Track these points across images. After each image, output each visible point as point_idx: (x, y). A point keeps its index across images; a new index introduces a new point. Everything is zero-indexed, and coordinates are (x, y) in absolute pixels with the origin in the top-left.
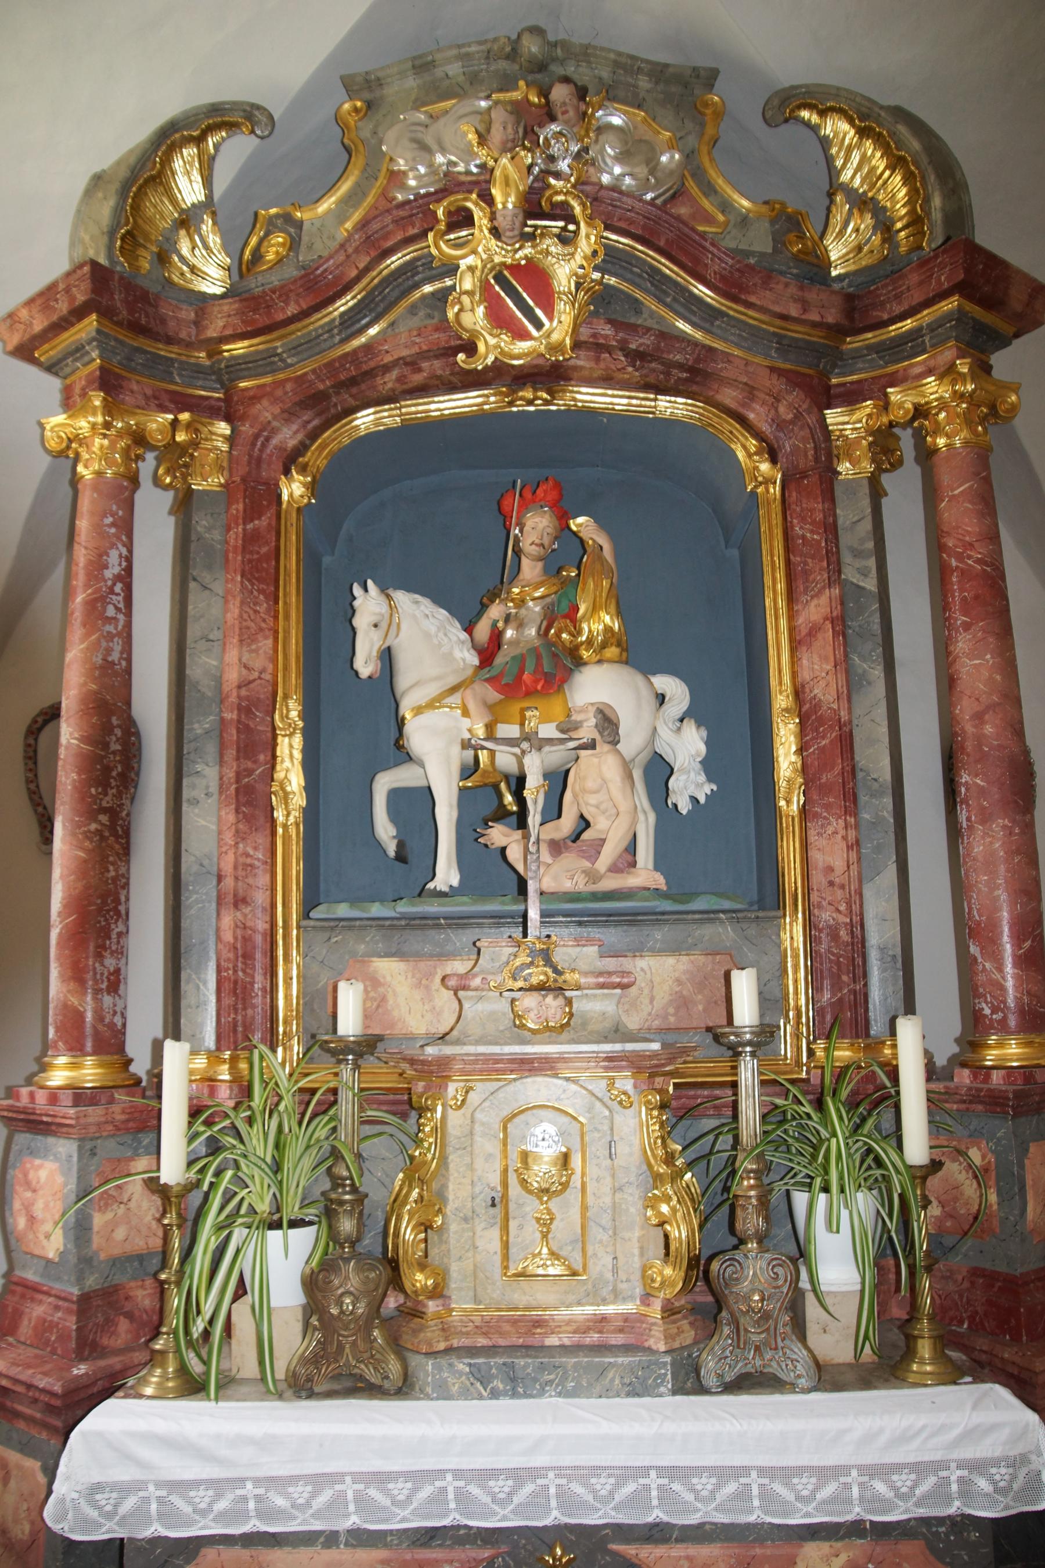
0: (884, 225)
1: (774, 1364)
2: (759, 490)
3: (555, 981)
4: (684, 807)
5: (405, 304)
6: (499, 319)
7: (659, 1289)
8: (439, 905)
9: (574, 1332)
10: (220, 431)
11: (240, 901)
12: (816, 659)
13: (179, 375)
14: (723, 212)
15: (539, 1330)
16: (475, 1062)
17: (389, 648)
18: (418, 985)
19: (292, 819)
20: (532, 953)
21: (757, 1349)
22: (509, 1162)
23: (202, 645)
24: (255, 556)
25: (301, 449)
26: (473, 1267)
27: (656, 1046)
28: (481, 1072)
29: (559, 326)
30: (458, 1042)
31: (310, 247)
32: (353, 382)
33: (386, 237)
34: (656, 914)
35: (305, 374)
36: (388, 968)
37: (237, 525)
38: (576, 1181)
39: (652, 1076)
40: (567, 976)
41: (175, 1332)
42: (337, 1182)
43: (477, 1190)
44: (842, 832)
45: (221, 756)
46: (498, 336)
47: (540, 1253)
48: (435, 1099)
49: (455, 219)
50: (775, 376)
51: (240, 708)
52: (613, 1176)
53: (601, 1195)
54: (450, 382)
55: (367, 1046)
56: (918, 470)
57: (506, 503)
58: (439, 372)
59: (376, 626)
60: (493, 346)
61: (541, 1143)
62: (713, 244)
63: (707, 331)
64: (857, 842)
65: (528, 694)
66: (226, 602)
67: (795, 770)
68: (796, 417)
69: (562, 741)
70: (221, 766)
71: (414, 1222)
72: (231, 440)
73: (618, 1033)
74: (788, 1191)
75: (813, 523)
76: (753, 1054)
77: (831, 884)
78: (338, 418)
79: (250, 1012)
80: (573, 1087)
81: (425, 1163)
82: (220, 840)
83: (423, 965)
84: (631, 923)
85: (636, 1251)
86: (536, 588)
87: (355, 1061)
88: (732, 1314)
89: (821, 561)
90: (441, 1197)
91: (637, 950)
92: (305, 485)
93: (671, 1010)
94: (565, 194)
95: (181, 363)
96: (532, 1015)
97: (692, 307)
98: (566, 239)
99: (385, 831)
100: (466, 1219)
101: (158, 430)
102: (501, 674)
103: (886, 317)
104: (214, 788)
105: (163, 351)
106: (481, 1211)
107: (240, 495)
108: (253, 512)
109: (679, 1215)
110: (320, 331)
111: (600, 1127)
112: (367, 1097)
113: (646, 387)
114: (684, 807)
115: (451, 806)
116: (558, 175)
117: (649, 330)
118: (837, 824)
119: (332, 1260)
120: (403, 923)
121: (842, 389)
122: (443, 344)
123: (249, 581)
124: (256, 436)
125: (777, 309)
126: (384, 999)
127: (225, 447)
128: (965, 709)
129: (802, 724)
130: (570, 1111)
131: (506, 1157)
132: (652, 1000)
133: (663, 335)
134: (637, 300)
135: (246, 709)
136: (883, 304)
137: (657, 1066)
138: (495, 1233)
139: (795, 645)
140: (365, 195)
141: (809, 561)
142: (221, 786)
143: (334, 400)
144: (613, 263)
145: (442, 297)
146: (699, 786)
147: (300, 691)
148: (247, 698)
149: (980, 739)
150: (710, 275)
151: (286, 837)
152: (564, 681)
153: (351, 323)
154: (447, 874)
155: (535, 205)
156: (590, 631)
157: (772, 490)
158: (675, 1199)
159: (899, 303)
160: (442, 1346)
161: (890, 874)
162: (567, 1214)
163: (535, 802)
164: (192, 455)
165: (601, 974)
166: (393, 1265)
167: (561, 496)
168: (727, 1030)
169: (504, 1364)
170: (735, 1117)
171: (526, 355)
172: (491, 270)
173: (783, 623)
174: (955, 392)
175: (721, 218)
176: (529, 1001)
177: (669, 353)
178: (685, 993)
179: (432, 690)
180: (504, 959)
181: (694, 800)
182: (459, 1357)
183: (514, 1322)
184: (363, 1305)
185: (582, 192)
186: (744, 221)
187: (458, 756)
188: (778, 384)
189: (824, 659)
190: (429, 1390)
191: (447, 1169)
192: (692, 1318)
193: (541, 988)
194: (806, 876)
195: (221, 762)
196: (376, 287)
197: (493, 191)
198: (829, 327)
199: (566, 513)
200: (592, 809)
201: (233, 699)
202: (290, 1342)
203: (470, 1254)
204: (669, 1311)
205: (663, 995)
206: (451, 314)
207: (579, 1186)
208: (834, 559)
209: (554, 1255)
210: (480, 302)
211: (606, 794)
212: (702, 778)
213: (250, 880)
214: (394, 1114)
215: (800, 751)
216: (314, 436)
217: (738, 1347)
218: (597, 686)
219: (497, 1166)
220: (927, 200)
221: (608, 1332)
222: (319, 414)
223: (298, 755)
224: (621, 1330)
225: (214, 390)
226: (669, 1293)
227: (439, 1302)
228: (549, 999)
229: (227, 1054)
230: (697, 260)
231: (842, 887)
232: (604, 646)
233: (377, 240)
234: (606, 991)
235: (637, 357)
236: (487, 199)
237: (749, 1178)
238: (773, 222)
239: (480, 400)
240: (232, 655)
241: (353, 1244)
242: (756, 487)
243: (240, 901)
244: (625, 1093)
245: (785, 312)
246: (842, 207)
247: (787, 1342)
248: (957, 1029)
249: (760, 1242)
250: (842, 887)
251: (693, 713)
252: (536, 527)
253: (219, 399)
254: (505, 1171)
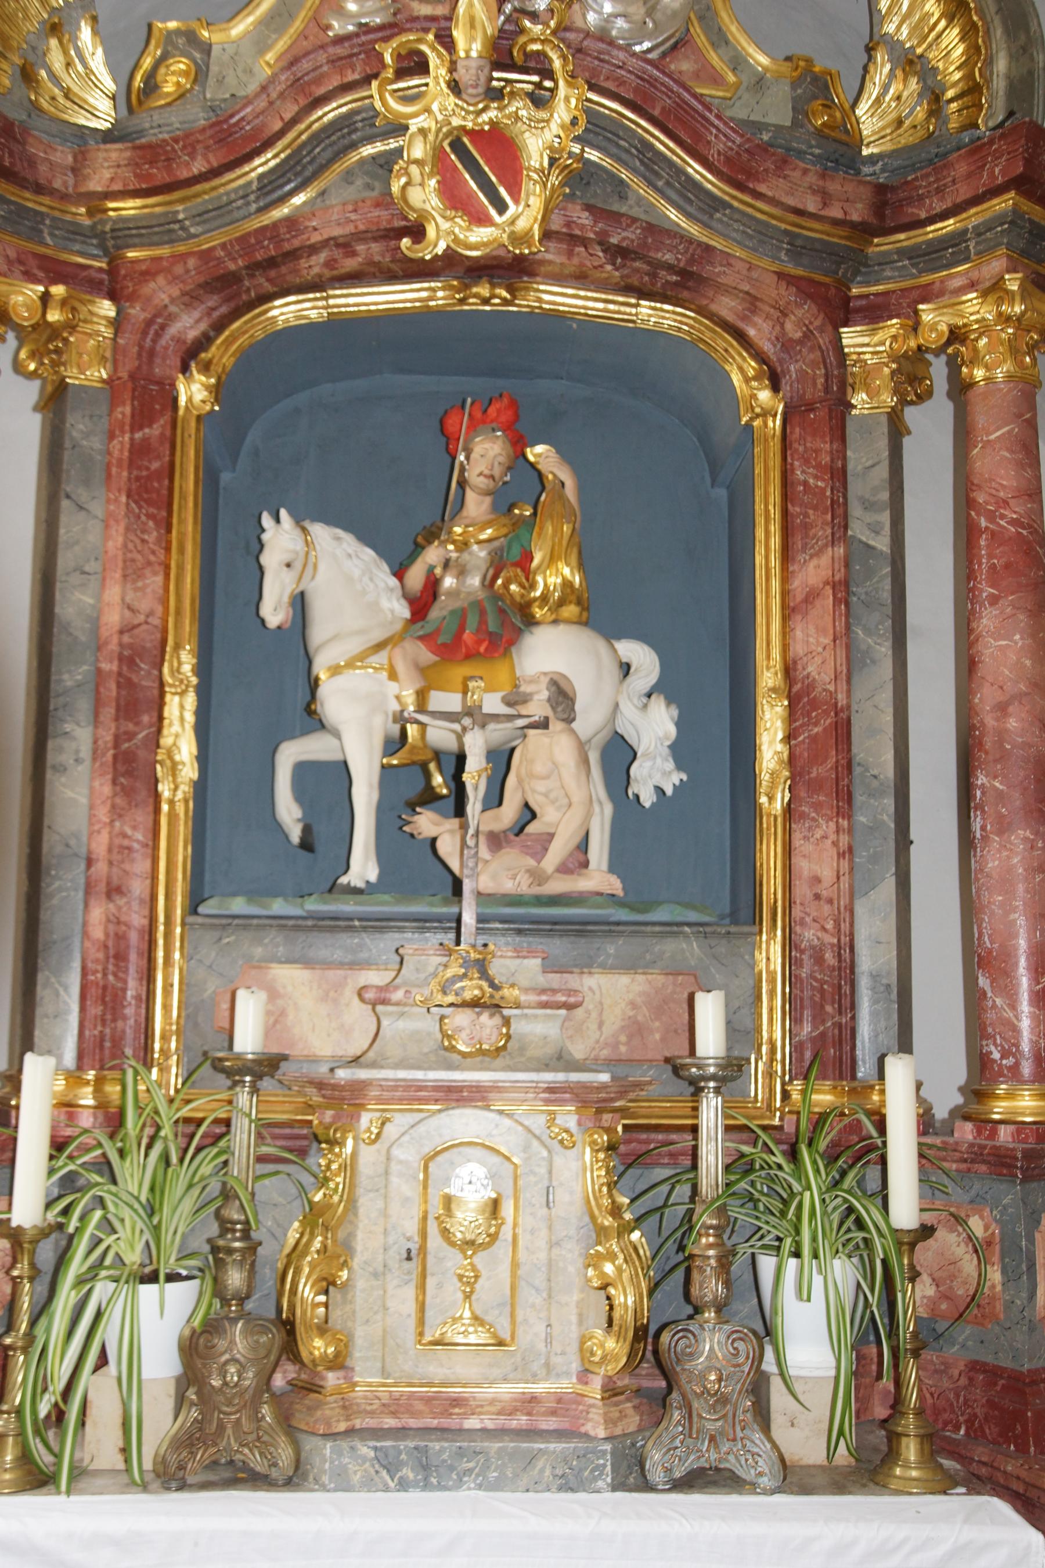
0: (934, 96)
1: (731, 1457)
2: (755, 424)
3: (492, 996)
4: (648, 799)
5: (339, 168)
6: (454, 199)
7: (600, 1364)
8: (356, 904)
9: (499, 1414)
10: (103, 312)
11: (114, 891)
12: (812, 630)
13: (51, 235)
14: (734, 70)
15: (457, 1410)
16: (395, 1088)
17: (302, 594)
18: (324, 998)
19: (180, 795)
20: (466, 963)
21: (712, 1439)
22: (430, 1209)
23: (76, 579)
24: (144, 473)
25: (204, 342)
26: (383, 1333)
27: (605, 1077)
28: (400, 1101)
29: (524, 214)
30: (373, 1065)
31: (220, 81)
32: (271, 263)
33: (318, 81)
34: (609, 923)
35: (212, 249)
36: (290, 977)
37: (123, 432)
38: (506, 1232)
39: (599, 1111)
40: (506, 992)
41: (19, 1411)
42: (226, 1226)
43: (391, 1240)
44: (833, 837)
45: (96, 714)
46: (452, 219)
47: (461, 1317)
48: (345, 1132)
49: (405, 64)
50: (784, 284)
51: (121, 658)
52: (550, 1228)
53: (534, 1250)
54: (389, 270)
55: (268, 1065)
56: (949, 407)
57: (451, 422)
58: (377, 258)
59: (288, 565)
60: (445, 232)
61: (467, 1187)
62: (719, 117)
63: (706, 225)
64: (850, 849)
65: (469, 656)
66: (107, 527)
67: (781, 762)
68: (805, 336)
69: (510, 718)
70: (96, 727)
71: (314, 1277)
72: (117, 324)
73: (561, 1061)
74: (753, 1255)
75: (818, 466)
76: (717, 1091)
77: (817, 897)
78: (251, 306)
79: (120, 1024)
80: (507, 1122)
81: (330, 1206)
82: (91, 817)
83: (333, 975)
84: (580, 933)
85: (574, 1319)
86: (483, 529)
87: (253, 1083)
88: (684, 1396)
89: (825, 513)
90: (348, 1248)
91: (586, 965)
92: (207, 387)
93: (623, 1038)
94: (543, 42)
95: (54, 219)
96: (464, 1035)
97: (688, 194)
98: (540, 100)
99: (289, 812)
100: (375, 1275)
101: (25, 305)
102: (437, 632)
103: (923, 215)
104: (86, 752)
105: (30, 201)
106: (394, 1264)
107: (127, 395)
108: (142, 418)
109: (625, 1276)
110: (233, 196)
111: (537, 1170)
112: (265, 1129)
113: (627, 289)
114: (648, 799)
115: (371, 786)
116: (534, 16)
117: (634, 220)
118: (826, 827)
119: (216, 1320)
120: (310, 923)
121: (864, 302)
122: (384, 225)
123: (136, 502)
124: (149, 323)
125: (791, 201)
126: (283, 1013)
127: (108, 332)
128: (986, 698)
129: (791, 708)
130: (503, 1150)
131: (426, 1202)
132: (601, 1025)
133: (651, 229)
134: (622, 182)
135: (128, 659)
136: (921, 198)
137: (605, 1100)
138: (410, 1293)
139: (788, 612)
140: (292, 17)
141: (811, 512)
142: (95, 751)
143: (247, 283)
144: (597, 134)
145: (386, 163)
146: (666, 774)
147: (195, 640)
148: (131, 646)
149: (1001, 735)
150: (712, 155)
151: (172, 815)
152: (512, 643)
153: (272, 189)
154: (363, 867)
155: (503, 54)
156: (546, 585)
157: (771, 424)
158: (621, 1257)
159: (942, 199)
160: (342, 1427)
161: (888, 887)
162: (494, 1269)
163: (476, 788)
164: (66, 341)
165: (543, 991)
166: (288, 1327)
167: (517, 417)
168: (688, 1061)
169: (416, 1448)
170: (695, 1167)
171: (485, 245)
172: (446, 136)
173: (775, 585)
174: (1000, 314)
175: (731, 78)
176: (462, 1019)
177: (658, 250)
178: (640, 1018)
179: (354, 646)
180: (431, 969)
181: (660, 791)
182: (363, 1439)
183: (428, 1400)
184: (251, 1375)
185: (563, 40)
186: (759, 83)
187: (382, 726)
188: (787, 295)
189: (821, 631)
190: (325, 1479)
191: (356, 1215)
192: (637, 1401)
193: (474, 1004)
194: (788, 886)
195: (96, 722)
196: (304, 145)
197: (455, 33)
198: (853, 226)
199: (522, 437)
200: (540, 799)
201: (113, 646)
202: (160, 1422)
203: (379, 1317)
204: (611, 1391)
205: (614, 1020)
206: (395, 188)
207: (510, 1239)
208: (840, 511)
209: (477, 1319)
210: (431, 175)
211: (557, 780)
212: (670, 765)
213: (127, 866)
214: (291, 1150)
215: (788, 738)
216: (219, 327)
217: (690, 1436)
218: (551, 651)
219: (416, 1213)
220: (989, 62)
221: (538, 1414)
222: (227, 300)
223: (190, 718)
224: (554, 1413)
225: (94, 257)
226: (612, 1368)
227: (340, 1374)
228: (485, 1017)
229: (91, 1075)
230: (698, 137)
231: (830, 901)
232: (561, 603)
233: (309, 84)
234: (549, 1011)
235: (619, 253)
236: (446, 41)
237: (709, 1235)
238: (795, 84)
239: (424, 294)
240: (113, 593)
241: (242, 1300)
242: (752, 419)
243: (114, 891)
244: (567, 1131)
245: (800, 206)
246: (882, 68)
247: (747, 1432)
248: (961, 1077)
249: (718, 1311)
250: (830, 901)
251: (664, 688)
252: (485, 455)
253: (100, 270)
254: (425, 1218)
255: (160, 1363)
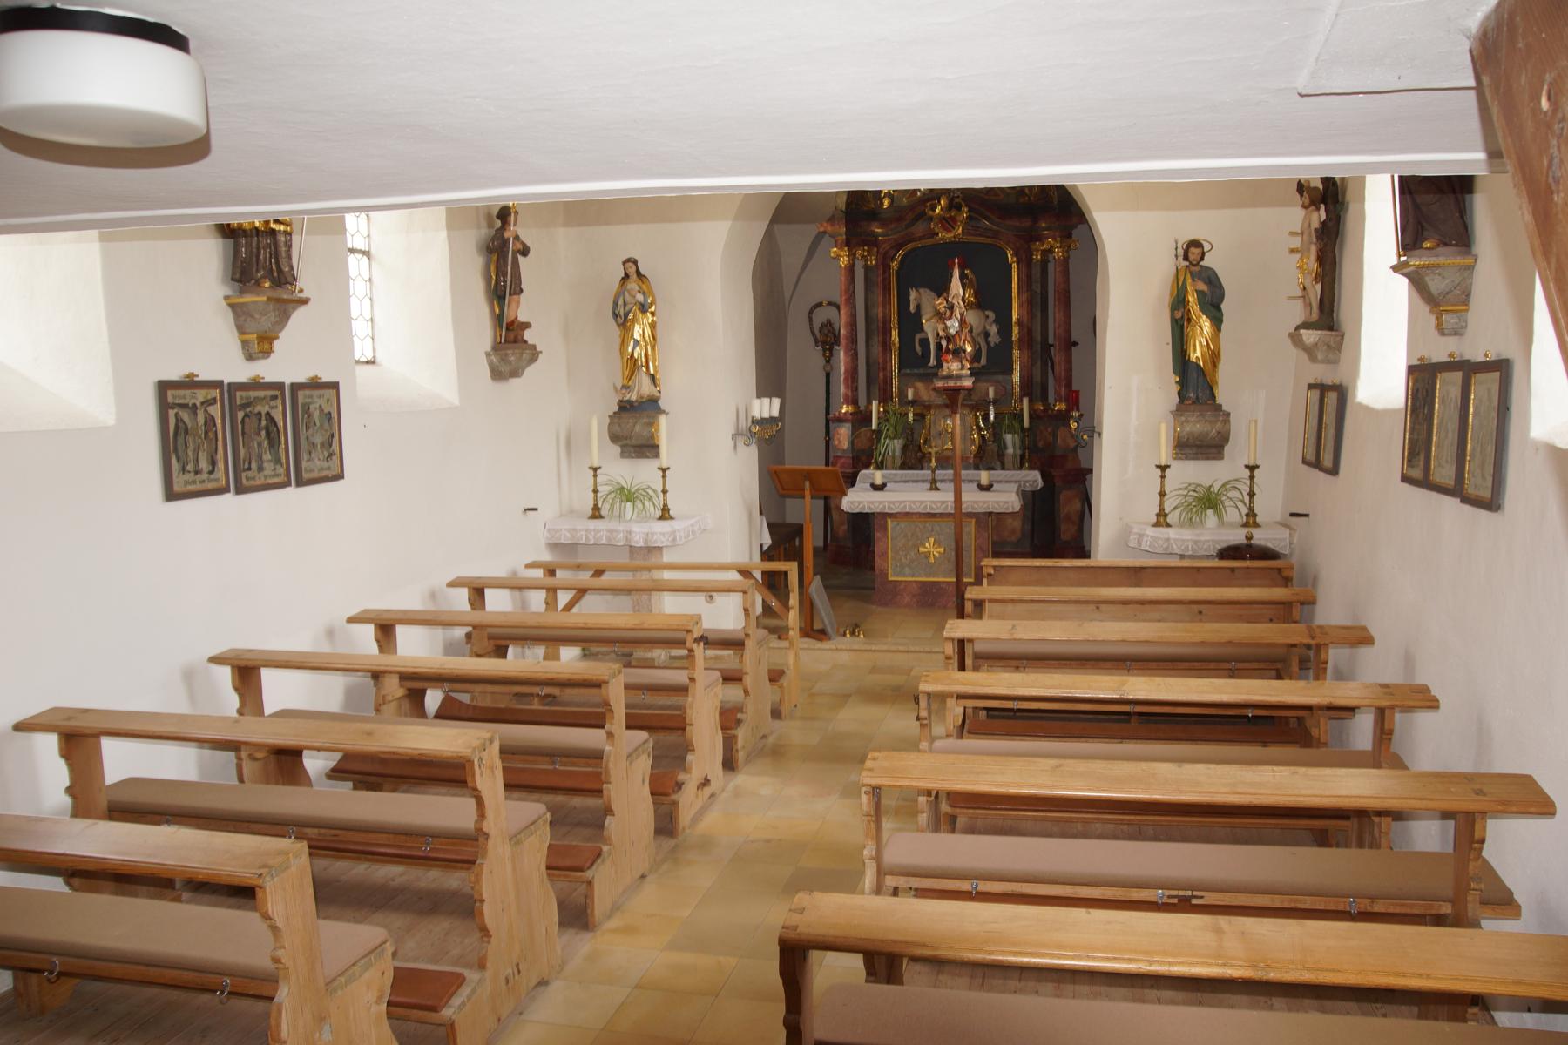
36: (920, 385)
139: (1020, 306)
202: (899, 462)
255: (898, 452)
